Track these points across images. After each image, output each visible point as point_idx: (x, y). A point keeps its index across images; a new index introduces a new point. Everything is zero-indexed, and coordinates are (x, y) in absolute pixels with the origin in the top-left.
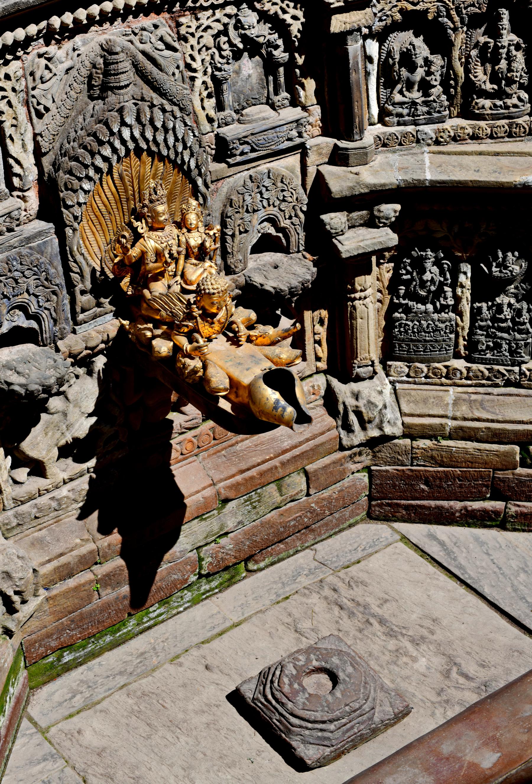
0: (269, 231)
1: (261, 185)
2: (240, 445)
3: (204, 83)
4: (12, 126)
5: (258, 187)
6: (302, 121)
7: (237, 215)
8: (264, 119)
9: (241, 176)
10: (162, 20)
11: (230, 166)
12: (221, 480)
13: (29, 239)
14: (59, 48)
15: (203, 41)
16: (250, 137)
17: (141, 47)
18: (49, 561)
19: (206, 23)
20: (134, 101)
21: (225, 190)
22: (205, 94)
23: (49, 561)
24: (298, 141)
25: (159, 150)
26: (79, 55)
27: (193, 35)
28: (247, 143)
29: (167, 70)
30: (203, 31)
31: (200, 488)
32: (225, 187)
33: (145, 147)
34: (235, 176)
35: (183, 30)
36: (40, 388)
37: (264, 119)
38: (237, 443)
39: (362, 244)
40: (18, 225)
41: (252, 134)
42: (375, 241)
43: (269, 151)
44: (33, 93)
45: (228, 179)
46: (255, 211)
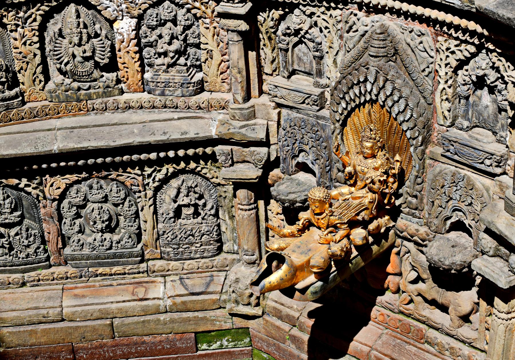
0: (464, 221)
1: (456, 182)
2: (411, 346)
3: (444, 89)
4: (330, 47)
5: (454, 182)
6: (494, 156)
7: (438, 191)
8: (477, 140)
9: (451, 168)
10: (428, 31)
11: (442, 155)
12: (377, 351)
13: (318, 117)
14: (367, 16)
15: (449, 60)
16: (458, 144)
17: (409, 40)
18: (276, 302)
19: (453, 48)
20: (376, 69)
21: (438, 170)
22: (444, 97)
23: (276, 302)
24: (490, 169)
25: (390, 111)
26: (373, 26)
27: (443, 51)
28: (453, 146)
29: (421, 66)
30: (450, 52)
31: (363, 342)
32: (439, 167)
33: (382, 104)
34: (446, 165)
35: (438, 45)
36: (278, 197)
37: (477, 140)
38: (410, 344)
39: (483, 268)
40: (314, 105)
41: (459, 143)
42: (492, 274)
43: (467, 163)
44: (346, 35)
45: (441, 164)
46: (451, 199)
